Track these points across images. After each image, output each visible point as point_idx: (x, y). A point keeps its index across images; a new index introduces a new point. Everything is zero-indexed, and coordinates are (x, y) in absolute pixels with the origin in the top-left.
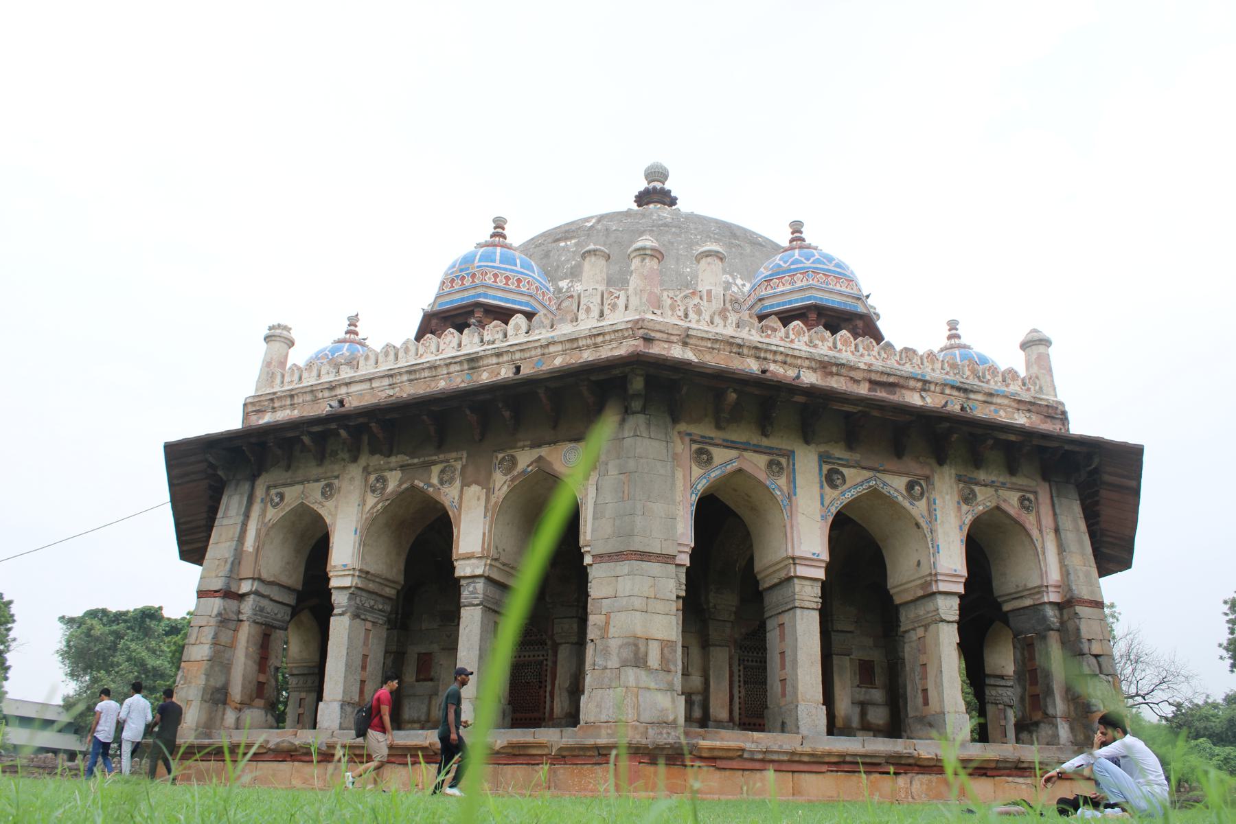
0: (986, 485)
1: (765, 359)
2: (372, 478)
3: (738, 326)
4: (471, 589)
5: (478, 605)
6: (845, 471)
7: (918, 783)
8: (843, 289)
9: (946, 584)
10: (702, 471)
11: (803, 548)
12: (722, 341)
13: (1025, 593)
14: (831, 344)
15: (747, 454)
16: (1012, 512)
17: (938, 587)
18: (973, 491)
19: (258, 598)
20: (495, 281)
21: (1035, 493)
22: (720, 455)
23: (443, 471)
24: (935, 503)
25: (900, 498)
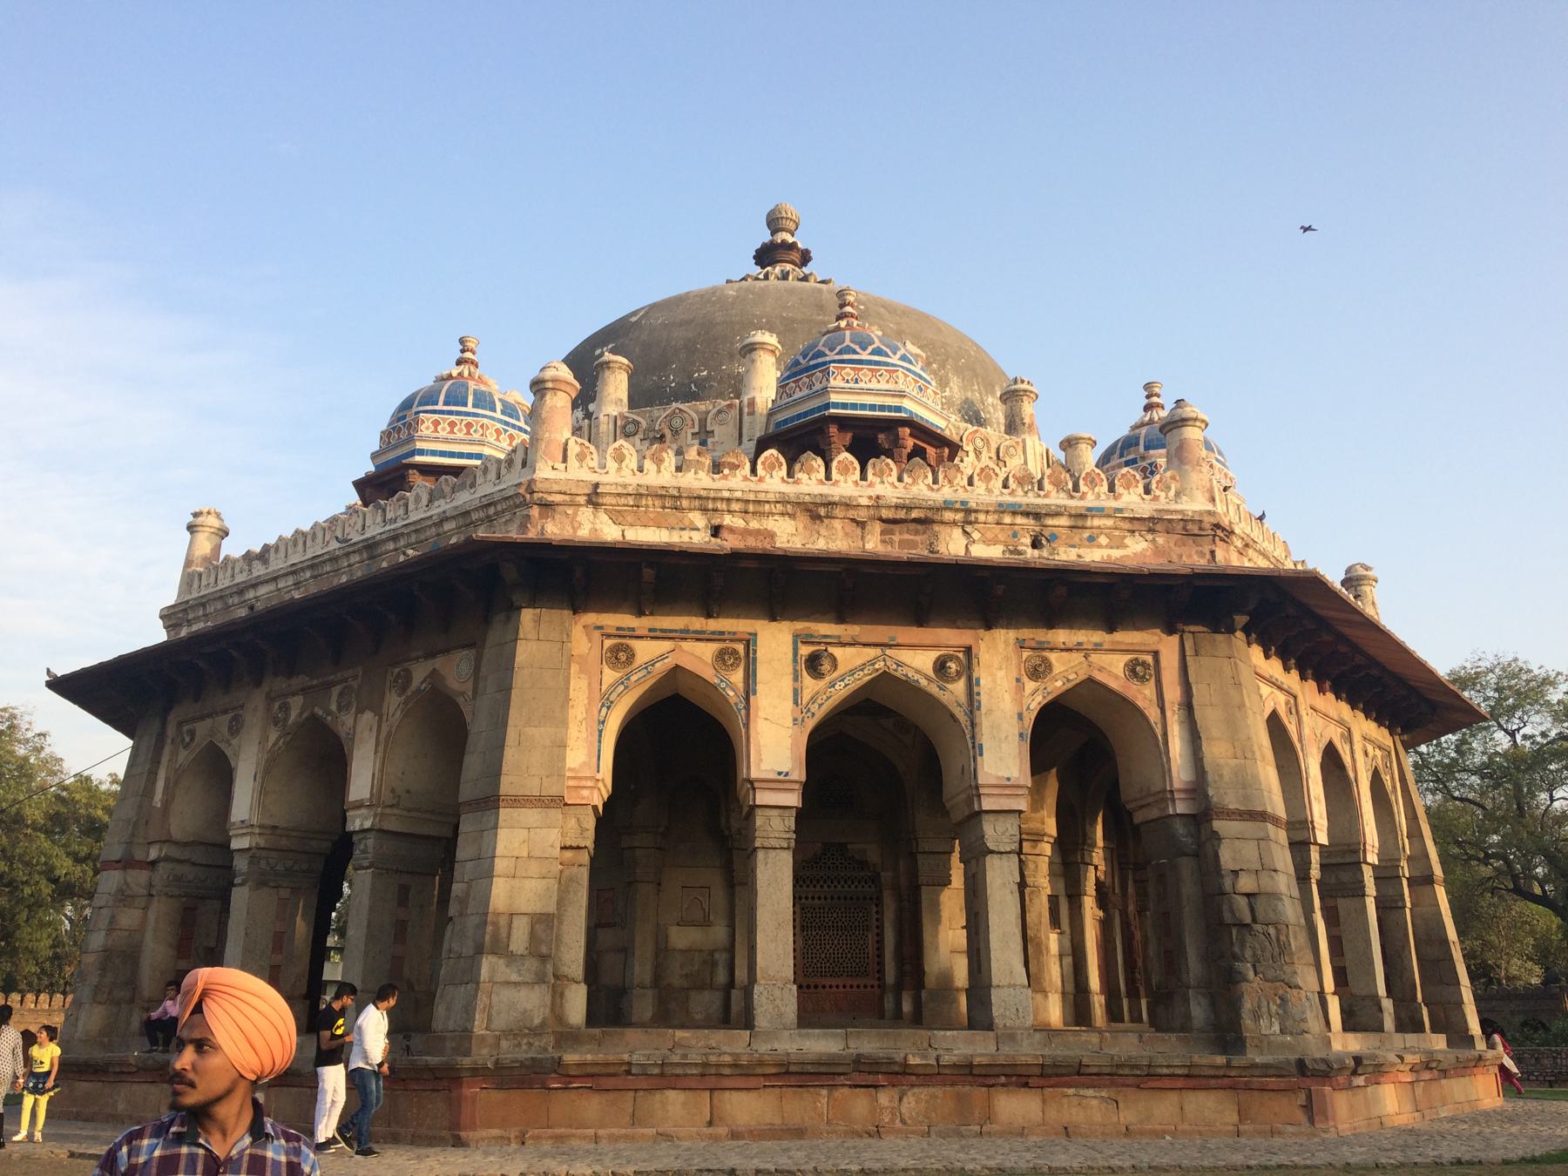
0: (1069, 650)
1: (715, 510)
2: (277, 705)
3: (679, 469)
4: (362, 847)
5: (367, 868)
6: (837, 652)
7: (912, 1099)
8: (883, 386)
9: (991, 800)
10: (617, 675)
11: (763, 767)
12: (648, 495)
13: (1151, 800)
14: (822, 475)
15: (687, 645)
16: (1113, 685)
17: (980, 804)
18: (1046, 661)
19: (170, 866)
20: (436, 431)
21: (1156, 654)
22: (645, 650)
23: (341, 694)
24: (978, 684)
25: (924, 682)
